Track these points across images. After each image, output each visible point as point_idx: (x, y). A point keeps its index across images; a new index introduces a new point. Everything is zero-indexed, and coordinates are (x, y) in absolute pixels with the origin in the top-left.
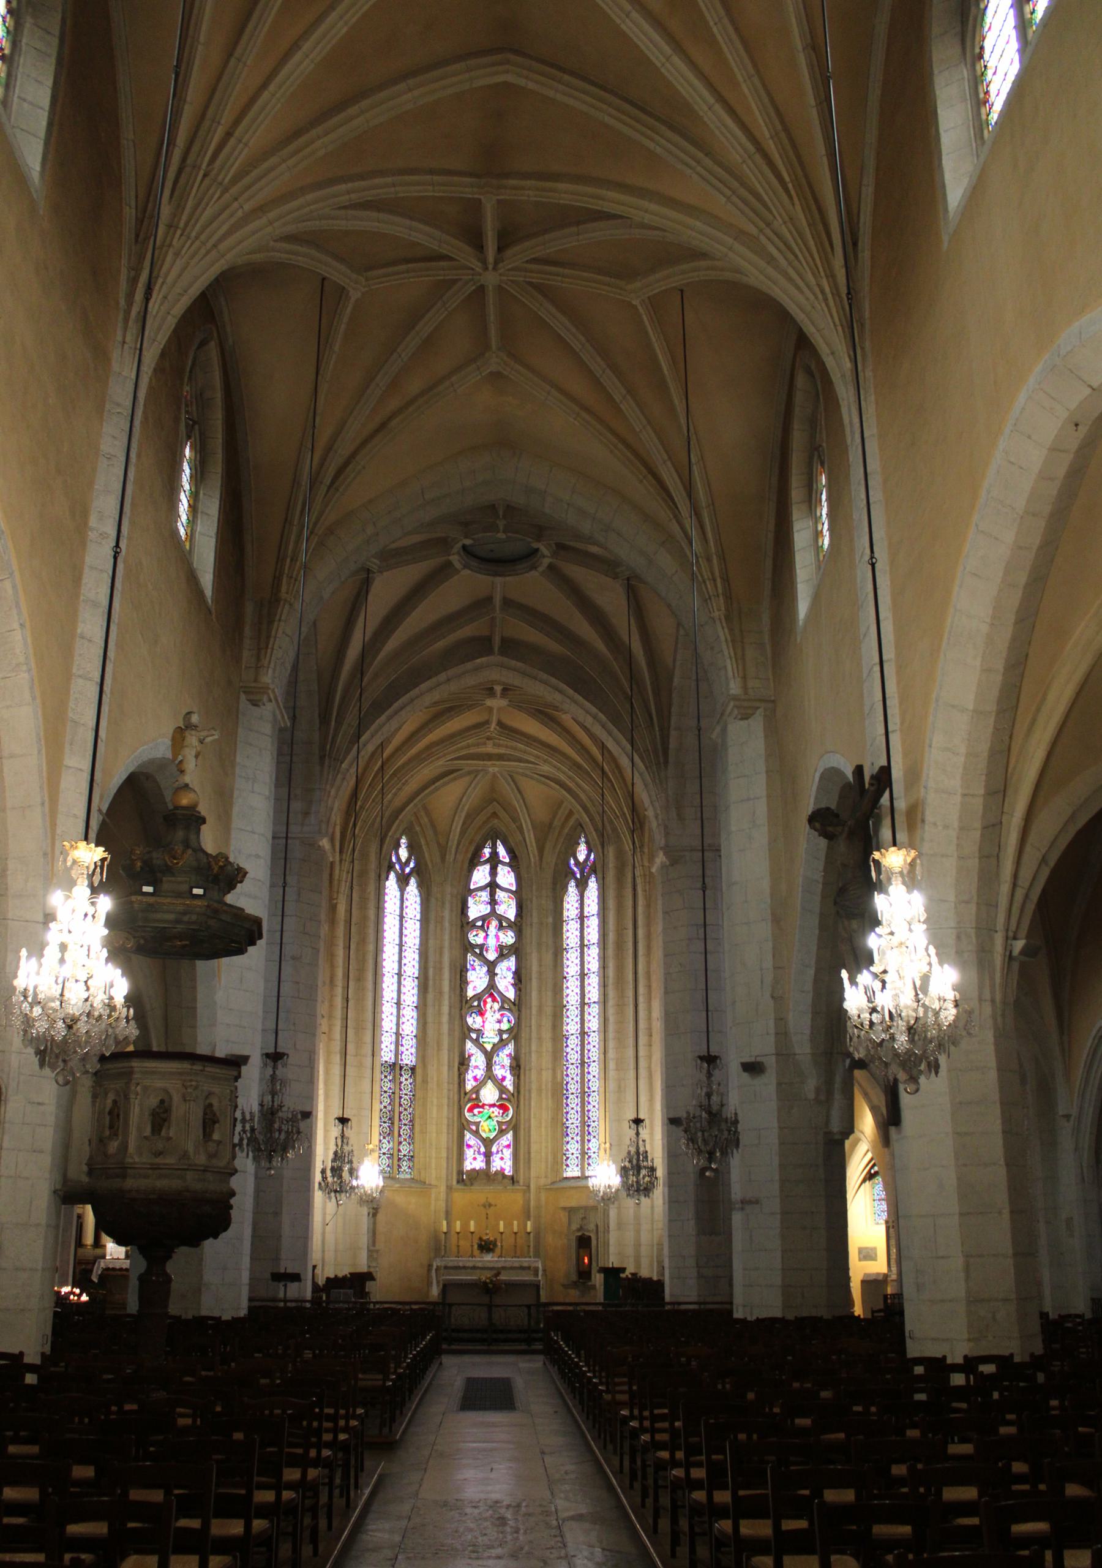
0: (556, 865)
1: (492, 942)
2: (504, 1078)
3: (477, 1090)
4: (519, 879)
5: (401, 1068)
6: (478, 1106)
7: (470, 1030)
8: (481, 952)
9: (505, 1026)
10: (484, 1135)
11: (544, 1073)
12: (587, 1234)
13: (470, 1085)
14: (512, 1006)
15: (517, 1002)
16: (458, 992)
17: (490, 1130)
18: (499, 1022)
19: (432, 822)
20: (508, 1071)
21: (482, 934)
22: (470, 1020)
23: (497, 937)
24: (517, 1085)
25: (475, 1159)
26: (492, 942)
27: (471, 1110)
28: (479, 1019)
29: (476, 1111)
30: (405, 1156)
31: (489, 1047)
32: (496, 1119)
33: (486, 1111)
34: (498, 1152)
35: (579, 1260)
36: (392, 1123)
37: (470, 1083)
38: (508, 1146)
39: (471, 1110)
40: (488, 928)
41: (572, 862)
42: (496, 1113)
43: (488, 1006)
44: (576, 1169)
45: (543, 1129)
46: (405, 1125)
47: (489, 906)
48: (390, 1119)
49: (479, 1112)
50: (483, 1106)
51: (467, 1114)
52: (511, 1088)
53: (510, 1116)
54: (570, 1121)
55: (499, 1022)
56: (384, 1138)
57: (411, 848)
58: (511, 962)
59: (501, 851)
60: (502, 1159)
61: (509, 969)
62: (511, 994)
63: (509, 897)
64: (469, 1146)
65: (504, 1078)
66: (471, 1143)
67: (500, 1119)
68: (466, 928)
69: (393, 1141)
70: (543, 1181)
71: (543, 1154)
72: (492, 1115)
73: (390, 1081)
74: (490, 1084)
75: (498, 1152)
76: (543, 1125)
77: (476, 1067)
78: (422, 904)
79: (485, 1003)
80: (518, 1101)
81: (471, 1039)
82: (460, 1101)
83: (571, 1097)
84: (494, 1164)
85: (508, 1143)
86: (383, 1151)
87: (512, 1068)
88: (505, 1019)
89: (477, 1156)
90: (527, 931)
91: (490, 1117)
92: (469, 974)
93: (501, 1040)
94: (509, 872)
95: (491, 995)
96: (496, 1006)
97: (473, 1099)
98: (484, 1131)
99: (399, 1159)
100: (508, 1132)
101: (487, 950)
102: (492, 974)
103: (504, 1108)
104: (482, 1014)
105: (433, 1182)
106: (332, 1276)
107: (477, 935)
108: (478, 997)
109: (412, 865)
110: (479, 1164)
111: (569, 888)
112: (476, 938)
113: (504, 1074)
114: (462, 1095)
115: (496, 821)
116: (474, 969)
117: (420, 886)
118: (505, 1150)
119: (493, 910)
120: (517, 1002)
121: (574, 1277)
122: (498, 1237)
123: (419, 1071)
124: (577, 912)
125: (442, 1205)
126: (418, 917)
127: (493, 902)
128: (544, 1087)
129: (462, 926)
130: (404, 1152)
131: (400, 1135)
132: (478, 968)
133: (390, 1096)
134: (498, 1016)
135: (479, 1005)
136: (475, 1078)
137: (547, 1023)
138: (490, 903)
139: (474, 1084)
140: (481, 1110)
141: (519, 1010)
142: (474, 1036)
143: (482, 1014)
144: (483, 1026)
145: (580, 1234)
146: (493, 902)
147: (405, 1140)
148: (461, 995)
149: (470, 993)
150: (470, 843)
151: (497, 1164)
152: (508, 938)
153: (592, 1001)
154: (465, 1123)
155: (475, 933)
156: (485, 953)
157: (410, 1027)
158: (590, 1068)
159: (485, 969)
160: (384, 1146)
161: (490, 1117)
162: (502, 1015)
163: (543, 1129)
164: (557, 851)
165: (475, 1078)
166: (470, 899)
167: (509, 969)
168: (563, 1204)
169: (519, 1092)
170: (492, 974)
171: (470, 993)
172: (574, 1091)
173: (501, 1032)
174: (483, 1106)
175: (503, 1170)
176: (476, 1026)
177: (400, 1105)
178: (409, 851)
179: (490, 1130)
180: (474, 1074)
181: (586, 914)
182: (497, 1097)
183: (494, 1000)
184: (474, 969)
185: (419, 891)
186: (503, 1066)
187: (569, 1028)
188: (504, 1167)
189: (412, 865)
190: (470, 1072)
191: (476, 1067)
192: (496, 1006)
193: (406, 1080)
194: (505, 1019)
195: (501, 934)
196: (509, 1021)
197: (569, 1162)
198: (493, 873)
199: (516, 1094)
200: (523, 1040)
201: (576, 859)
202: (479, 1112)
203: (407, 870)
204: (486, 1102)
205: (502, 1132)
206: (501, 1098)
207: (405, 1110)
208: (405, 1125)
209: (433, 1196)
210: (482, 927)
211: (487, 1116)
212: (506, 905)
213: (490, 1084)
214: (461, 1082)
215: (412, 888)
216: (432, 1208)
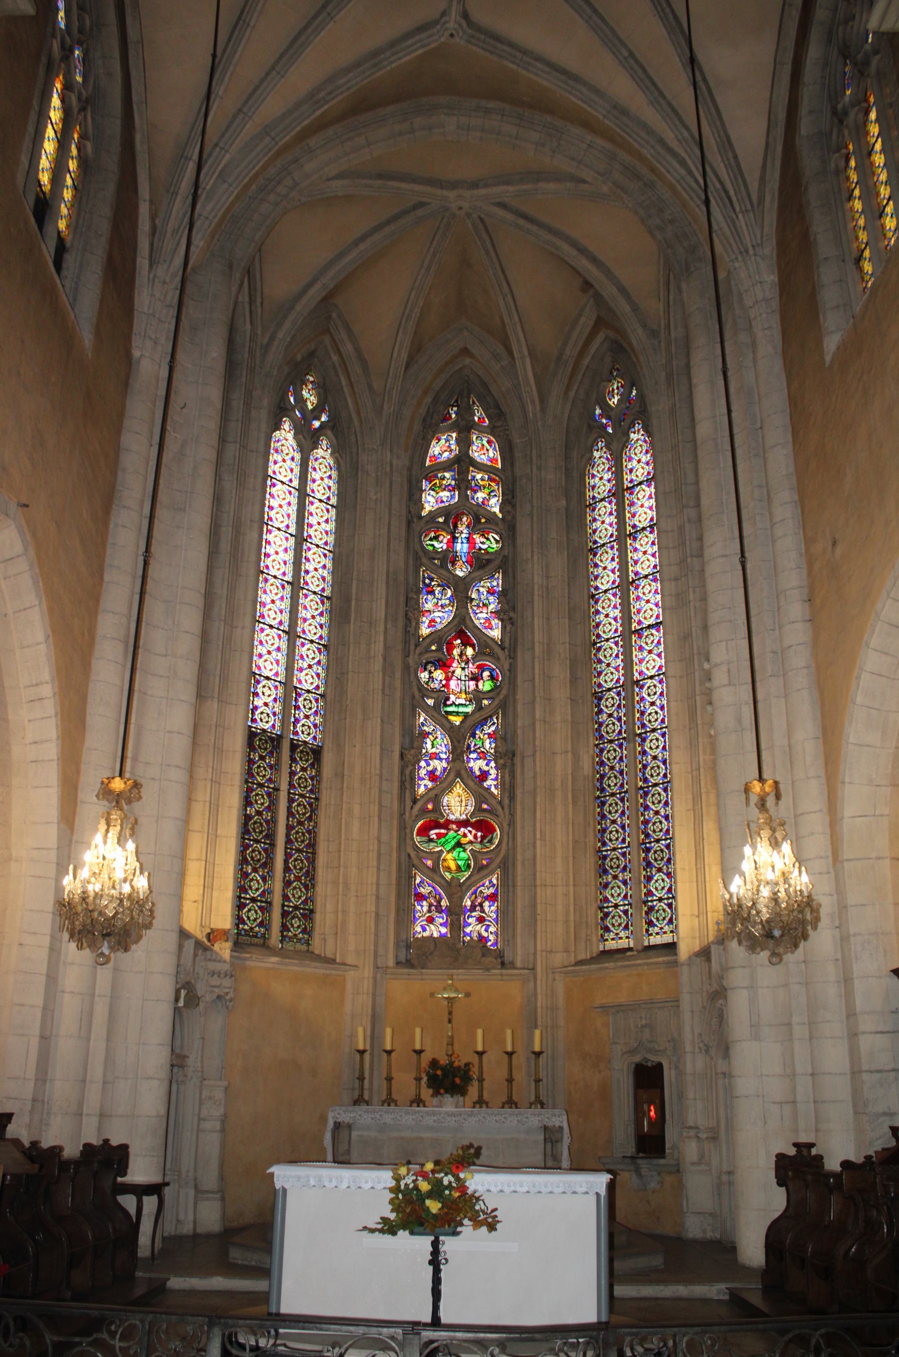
0: (569, 418)
1: (461, 547)
2: (484, 775)
3: (436, 798)
4: (507, 452)
5: (294, 747)
6: (438, 825)
7: (424, 691)
8: (443, 566)
9: (486, 686)
10: (448, 876)
11: (559, 759)
12: (654, 1058)
13: (424, 786)
14: (498, 650)
15: (507, 644)
16: (401, 623)
17: (458, 867)
18: (476, 678)
19: (358, 350)
20: (493, 764)
21: (446, 538)
22: (424, 676)
23: (470, 540)
24: (509, 787)
25: (431, 920)
26: (461, 547)
27: (424, 831)
28: (439, 675)
29: (433, 833)
30: (296, 908)
31: (457, 720)
32: (469, 848)
33: (452, 834)
34: (473, 908)
35: (639, 1113)
36: (273, 845)
37: (422, 783)
38: (492, 898)
39: (424, 831)
40: (456, 527)
41: (598, 412)
42: (470, 837)
43: (456, 652)
44: (622, 934)
45: (559, 861)
46: (298, 850)
47: (457, 493)
48: (267, 836)
49: (439, 836)
50: (446, 825)
51: (417, 839)
52: (495, 792)
53: (497, 841)
54: (610, 846)
55: (476, 678)
56: (255, 870)
57: (323, 390)
58: (497, 582)
59: (478, 414)
60: (481, 920)
61: (491, 592)
62: (496, 633)
63: (490, 479)
64: (420, 897)
65: (484, 775)
66: (424, 891)
67: (477, 847)
68: (417, 526)
69: (272, 878)
70: (559, 959)
71: (560, 908)
72: (464, 841)
73: (271, 767)
74: (459, 789)
75: (473, 908)
76: (559, 854)
77: (435, 756)
78: (340, 482)
79: (451, 647)
80: (512, 815)
81: (426, 708)
82: (402, 814)
83: (611, 800)
84: (468, 930)
85: (492, 890)
86: (252, 894)
87: (498, 756)
88: (486, 674)
89: (435, 914)
90: (524, 527)
91: (459, 844)
92: (423, 597)
93: (479, 708)
94: (489, 442)
95: (461, 634)
96: (470, 651)
97: (430, 811)
98: (448, 869)
99: (284, 914)
100: (492, 873)
101: (453, 563)
102: (462, 598)
103: (484, 828)
104: (444, 665)
105: (350, 960)
106: (95, 1141)
107: (436, 538)
108: (437, 637)
109: (324, 418)
110: (437, 930)
111: (596, 454)
112: (435, 543)
113: (486, 768)
114: (408, 803)
115: (467, 361)
116: (432, 592)
117: (338, 451)
118: (486, 904)
119: (464, 497)
120: (507, 644)
121: (631, 1150)
122: (475, 1059)
123: (328, 758)
124: (608, 486)
125: (364, 1001)
126: (333, 501)
127: (463, 485)
128: (558, 784)
129: (409, 523)
130: (294, 902)
131: (287, 869)
132: (437, 590)
133: (269, 795)
134: (472, 668)
135: (439, 649)
136: (432, 775)
137: (560, 672)
138: (459, 489)
139: (430, 785)
140: (443, 831)
141: (512, 656)
142: (430, 702)
143: (444, 665)
144: (447, 686)
145: (637, 1059)
146: (463, 485)
147: (298, 879)
148: (406, 632)
149: (425, 631)
150: (425, 392)
151: (473, 928)
152: (490, 543)
153: (646, 623)
154: (413, 854)
155: (432, 534)
156: (449, 566)
157: (307, 680)
158: (647, 744)
159: (449, 593)
160: (254, 885)
161: (459, 844)
162: (481, 668)
163: (559, 861)
164: (572, 394)
165: (432, 775)
166: (425, 484)
167: (491, 592)
168: (600, 1000)
169: (512, 798)
170: (462, 598)
171: (425, 631)
172: (615, 789)
173: (476, 697)
174: (446, 825)
175: (482, 939)
176: (435, 685)
177: (290, 814)
178: (318, 395)
179: (458, 867)
180: (430, 768)
181: (627, 484)
182: (471, 809)
183: (466, 642)
184: (432, 592)
185: (337, 461)
186: (483, 755)
187: (601, 680)
188: (485, 934)
189: (324, 418)
190: (423, 764)
191: (435, 756)
192: (470, 651)
193: (303, 769)
194: (486, 674)
195: (478, 538)
196: (492, 678)
197: (608, 922)
198: (465, 443)
199: (506, 801)
200: (520, 707)
201: (605, 407)
202: (439, 836)
203: (316, 424)
204: (452, 817)
205: (480, 870)
206: (478, 809)
207: (300, 823)
208: (298, 850)
209: (349, 986)
210: (444, 526)
211: (453, 843)
212: (487, 491)
213: (459, 789)
214: (408, 780)
215: (323, 454)
216: (348, 1008)
